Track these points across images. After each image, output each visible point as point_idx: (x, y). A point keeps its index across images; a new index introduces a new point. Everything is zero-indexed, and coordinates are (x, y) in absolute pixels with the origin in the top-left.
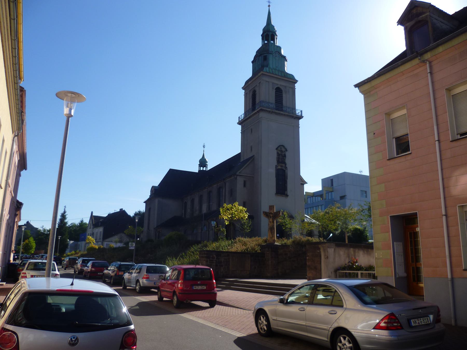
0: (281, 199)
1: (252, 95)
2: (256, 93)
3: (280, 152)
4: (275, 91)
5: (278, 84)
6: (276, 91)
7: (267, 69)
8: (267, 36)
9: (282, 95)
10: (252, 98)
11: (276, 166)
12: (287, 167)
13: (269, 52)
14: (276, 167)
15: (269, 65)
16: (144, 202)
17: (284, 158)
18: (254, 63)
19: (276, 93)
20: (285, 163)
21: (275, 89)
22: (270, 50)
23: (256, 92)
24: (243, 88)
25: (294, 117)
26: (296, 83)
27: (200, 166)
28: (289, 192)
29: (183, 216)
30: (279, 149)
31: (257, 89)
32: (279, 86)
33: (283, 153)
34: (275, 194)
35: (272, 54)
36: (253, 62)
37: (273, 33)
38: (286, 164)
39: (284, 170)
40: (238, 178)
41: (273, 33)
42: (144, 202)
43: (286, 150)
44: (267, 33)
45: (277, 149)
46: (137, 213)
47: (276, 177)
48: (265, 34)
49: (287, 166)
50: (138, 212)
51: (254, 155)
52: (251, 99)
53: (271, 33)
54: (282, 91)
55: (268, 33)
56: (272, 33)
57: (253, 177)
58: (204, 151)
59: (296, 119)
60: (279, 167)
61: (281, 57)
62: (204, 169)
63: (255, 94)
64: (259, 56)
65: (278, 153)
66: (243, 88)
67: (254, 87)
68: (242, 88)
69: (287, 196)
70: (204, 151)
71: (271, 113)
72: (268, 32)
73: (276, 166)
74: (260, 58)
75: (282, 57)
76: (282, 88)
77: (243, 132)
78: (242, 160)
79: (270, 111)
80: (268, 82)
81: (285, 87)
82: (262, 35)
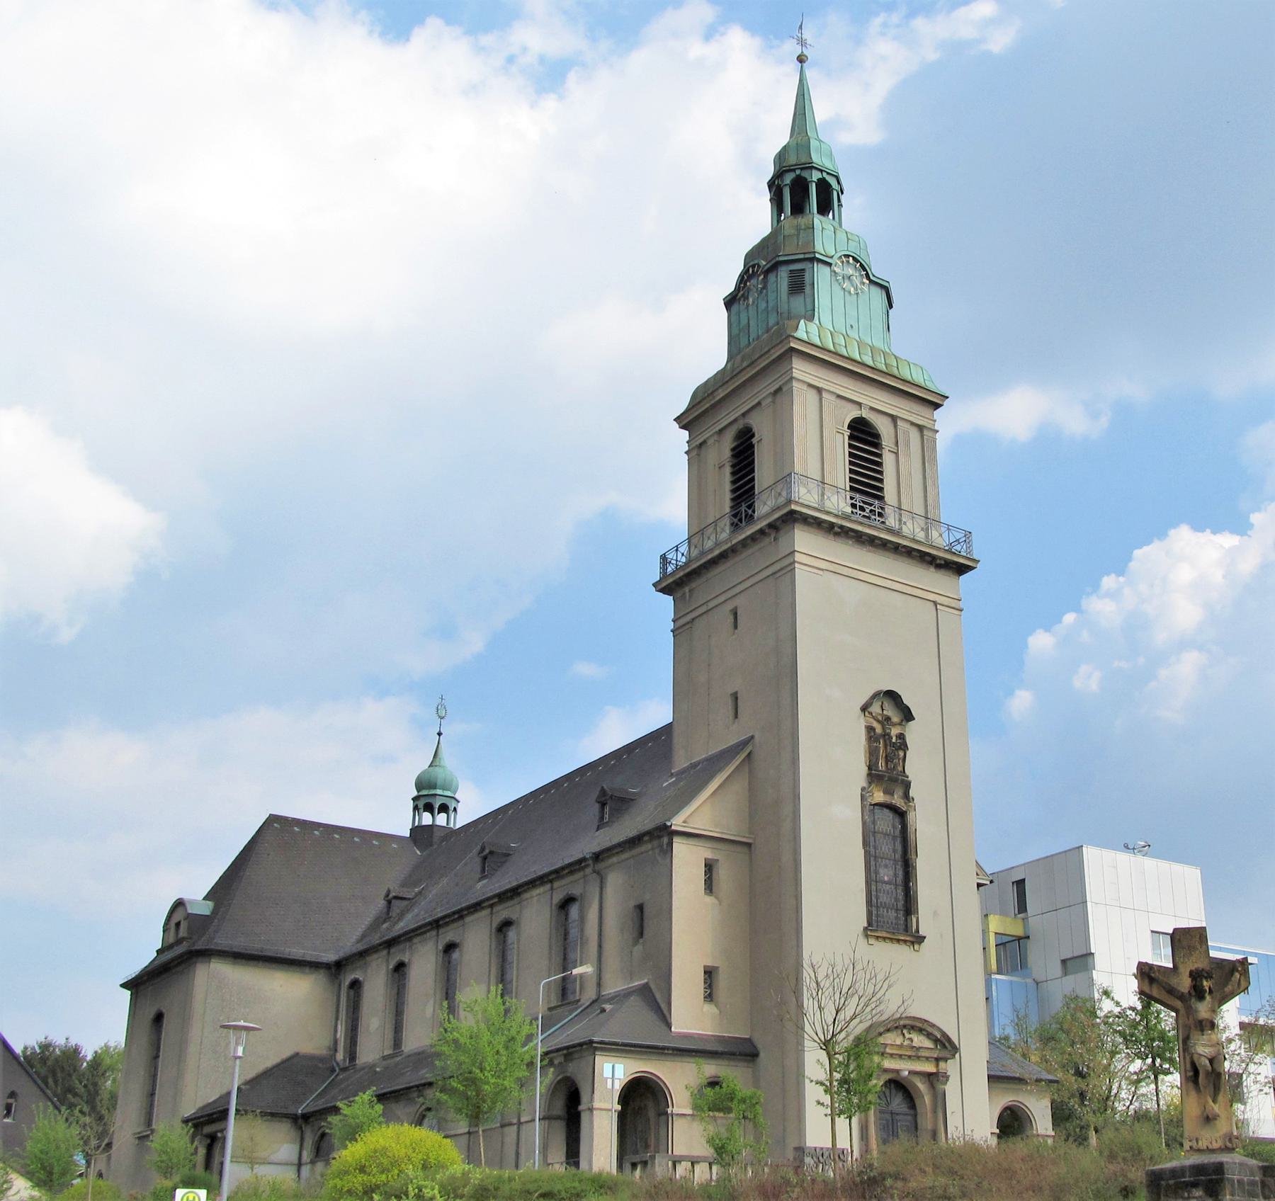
0: (888, 955)
1: (733, 450)
2: (754, 441)
3: (879, 730)
4: (847, 433)
5: (860, 404)
6: (851, 437)
7: (813, 328)
8: (800, 187)
9: (880, 456)
10: (733, 466)
13: (817, 256)
14: (862, 797)
15: (816, 310)
16: (121, 986)
17: (901, 754)
18: (735, 308)
20: (908, 777)
21: (849, 427)
22: (819, 248)
23: (753, 436)
24: (687, 421)
25: (938, 561)
26: (937, 406)
27: (421, 804)
28: (927, 919)
29: (340, 1056)
30: (875, 708)
31: (762, 426)
32: (865, 414)
33: (894, 731)
34: (865, 929)
35: (830, 265)
36: (730, 302)
38: (907, 786)
40: (680, 848)
41: (825, 174)
42: (121, 986)
43: (907, 715)
44: (798, 172)
45: (864, 709)
46: (34, 1053)
47: (866, 843)
48: (788, 178)
50: (38, 1051)
51: (752, 737)
52: (728, 470)
53: (816, 176)
54: (877, 436)
55: (805, 174)
56: (820, 176)
57: (749, 845)
58: (440, 734)
59: (943, 571)
60: (879, 797)
61: (868, 282)
62: (441, 819)
63: (752, 446)
64: (767, 272)
65: (870, 729)
66: (687, 421)
67: (744, 415)
68: (677, 420)
69: (921, 939)
70: (440, 734)
71: (837, 534)
72: (802, 169)
73: (863, 789)
74: (772, 277)
75: (871, 281)
76: (883, 426)
77: (681, 629)
78: (681, 761)
79: (832, 525)
80: (819, 390)
81: (894, 419)
82: (771, 184)
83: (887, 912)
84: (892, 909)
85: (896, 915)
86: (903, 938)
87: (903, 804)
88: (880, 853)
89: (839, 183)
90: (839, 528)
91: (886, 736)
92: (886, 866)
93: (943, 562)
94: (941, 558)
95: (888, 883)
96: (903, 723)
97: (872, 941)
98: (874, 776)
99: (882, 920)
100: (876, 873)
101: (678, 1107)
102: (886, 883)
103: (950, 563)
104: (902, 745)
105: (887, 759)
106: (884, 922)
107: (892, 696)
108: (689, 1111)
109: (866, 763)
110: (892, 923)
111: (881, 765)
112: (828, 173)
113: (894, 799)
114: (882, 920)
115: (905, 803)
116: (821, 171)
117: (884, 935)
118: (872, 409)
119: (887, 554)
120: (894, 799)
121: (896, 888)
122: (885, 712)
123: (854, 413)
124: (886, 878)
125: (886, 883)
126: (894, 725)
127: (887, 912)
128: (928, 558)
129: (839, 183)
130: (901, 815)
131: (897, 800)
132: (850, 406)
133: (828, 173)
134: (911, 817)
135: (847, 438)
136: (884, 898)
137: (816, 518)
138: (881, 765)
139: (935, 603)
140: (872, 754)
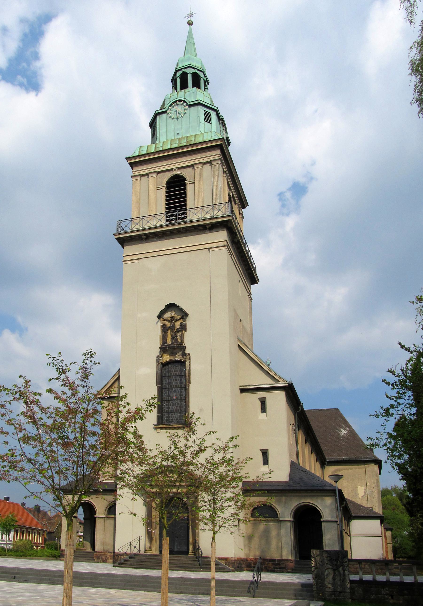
3: (168, 324)
5: (172, 170)
9: (185, 189)
11: (159, 358)
12: (189, 354)
14: (157, 361)
19: (167, 192)
21: (168, 183)
32: (175, 173)
37: (184, 70)
38: (183, 348)
39: (184, 363)
45: (160, 316)
49: (187, 352)
56: (181, 72)
60: (167, 358)
61: (187, 107)
73: (158, 356)
83: (175, 414)
84: (177, 412)
85: (180, 415)
86: (176, 426)
87: (182, 358)
88: (171, 386)
89: (194, 69)
90: (144, 236)
91: (172, 327)
92: (175, 391)
93: (210, 226)
94: (208, 224)
95: (177, 399)
96: (185, 317)
97: (159, 430)
98: (164, 349)
99: (171, 419)
100: (169, 396)
101: (99, 514)
102: (175, 400)
103: (215, 224)
104: (183, 327)
105: (172, 338)
106: (172, 420)
107: (171, 307)
108: (103, 516)
109: (160, 344)
110: (177, 419)
111: (169, 342)
112: (185, 68)
113: (176, 357)
114: (171, 419)
115: (183, 357)
116: (181, 70)
117: (165, 426)
118: (179, 168)
119: (178, 235)
120: (176, 357)
121: (181, 402)
122: (173, 315)
123: (169, 175)
124: (175, 398)
125: (175, 400)
126: (177, 320)
127: (175, 414)
128: (201, 228)
129: (194, 69)
130: (183, 363)
131: (178, 357)
132: (167, 173)
133: (185, 68)
134: (187, 363)
135: (164, 190)
136: (173, 408)
137: (130, 237)
138: (169, 342)
139: (209, 249)
140: (164, 337)
